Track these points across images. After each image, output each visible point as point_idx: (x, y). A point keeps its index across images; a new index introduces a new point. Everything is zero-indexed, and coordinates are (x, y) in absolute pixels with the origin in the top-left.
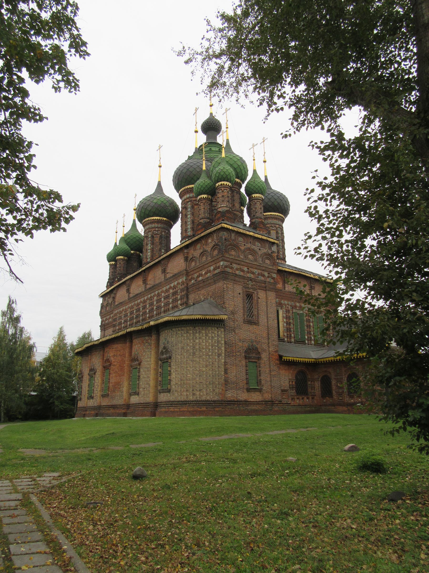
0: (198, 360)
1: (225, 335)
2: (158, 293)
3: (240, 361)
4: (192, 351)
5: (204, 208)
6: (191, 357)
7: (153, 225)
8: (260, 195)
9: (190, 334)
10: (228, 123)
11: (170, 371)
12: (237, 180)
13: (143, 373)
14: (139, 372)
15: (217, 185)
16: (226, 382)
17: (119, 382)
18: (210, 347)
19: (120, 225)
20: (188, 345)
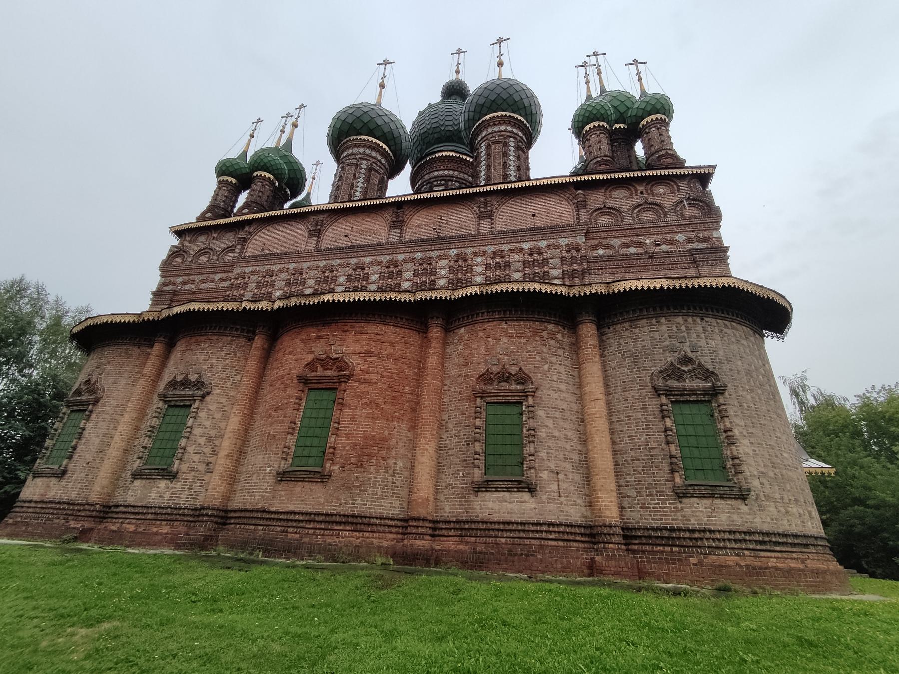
7: (373, 154)
17: (385, 440)
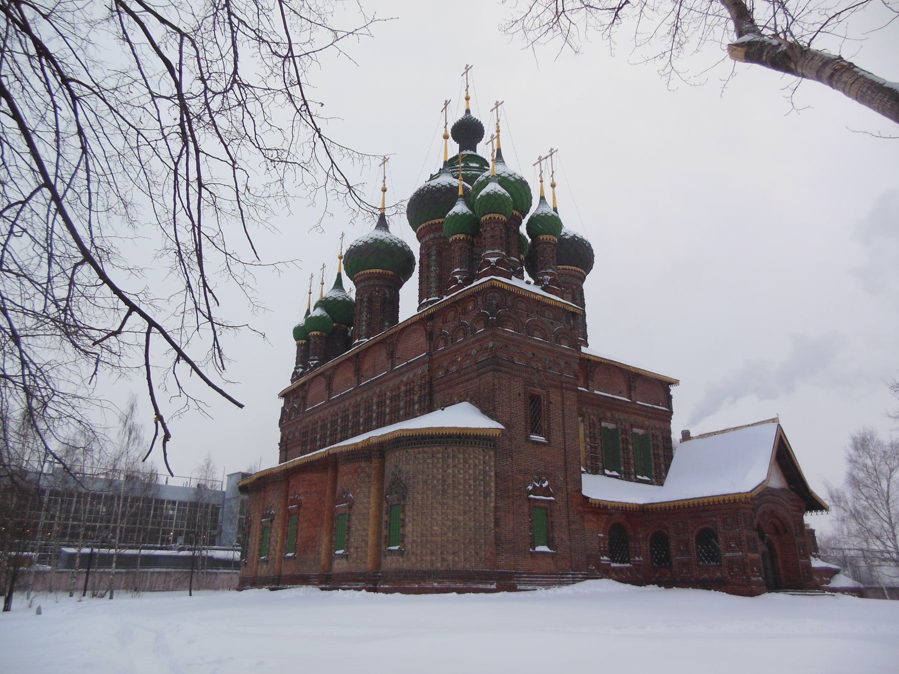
0: (451, 502)
1: (495, 463)
2: (381, 391)
4: (440, 487)
5: (461, 256)
6: (439, 497)
8: (552, 237)
9: (438, 459)
10: (500, 124)
11: (404, 520)
12: (515, 212)
13: (356, 522)
14: (349, 520)
15: (483, 218)
16: (498, 541)
18: (471, 482)
19: (317, 281)
20: (433, 477)
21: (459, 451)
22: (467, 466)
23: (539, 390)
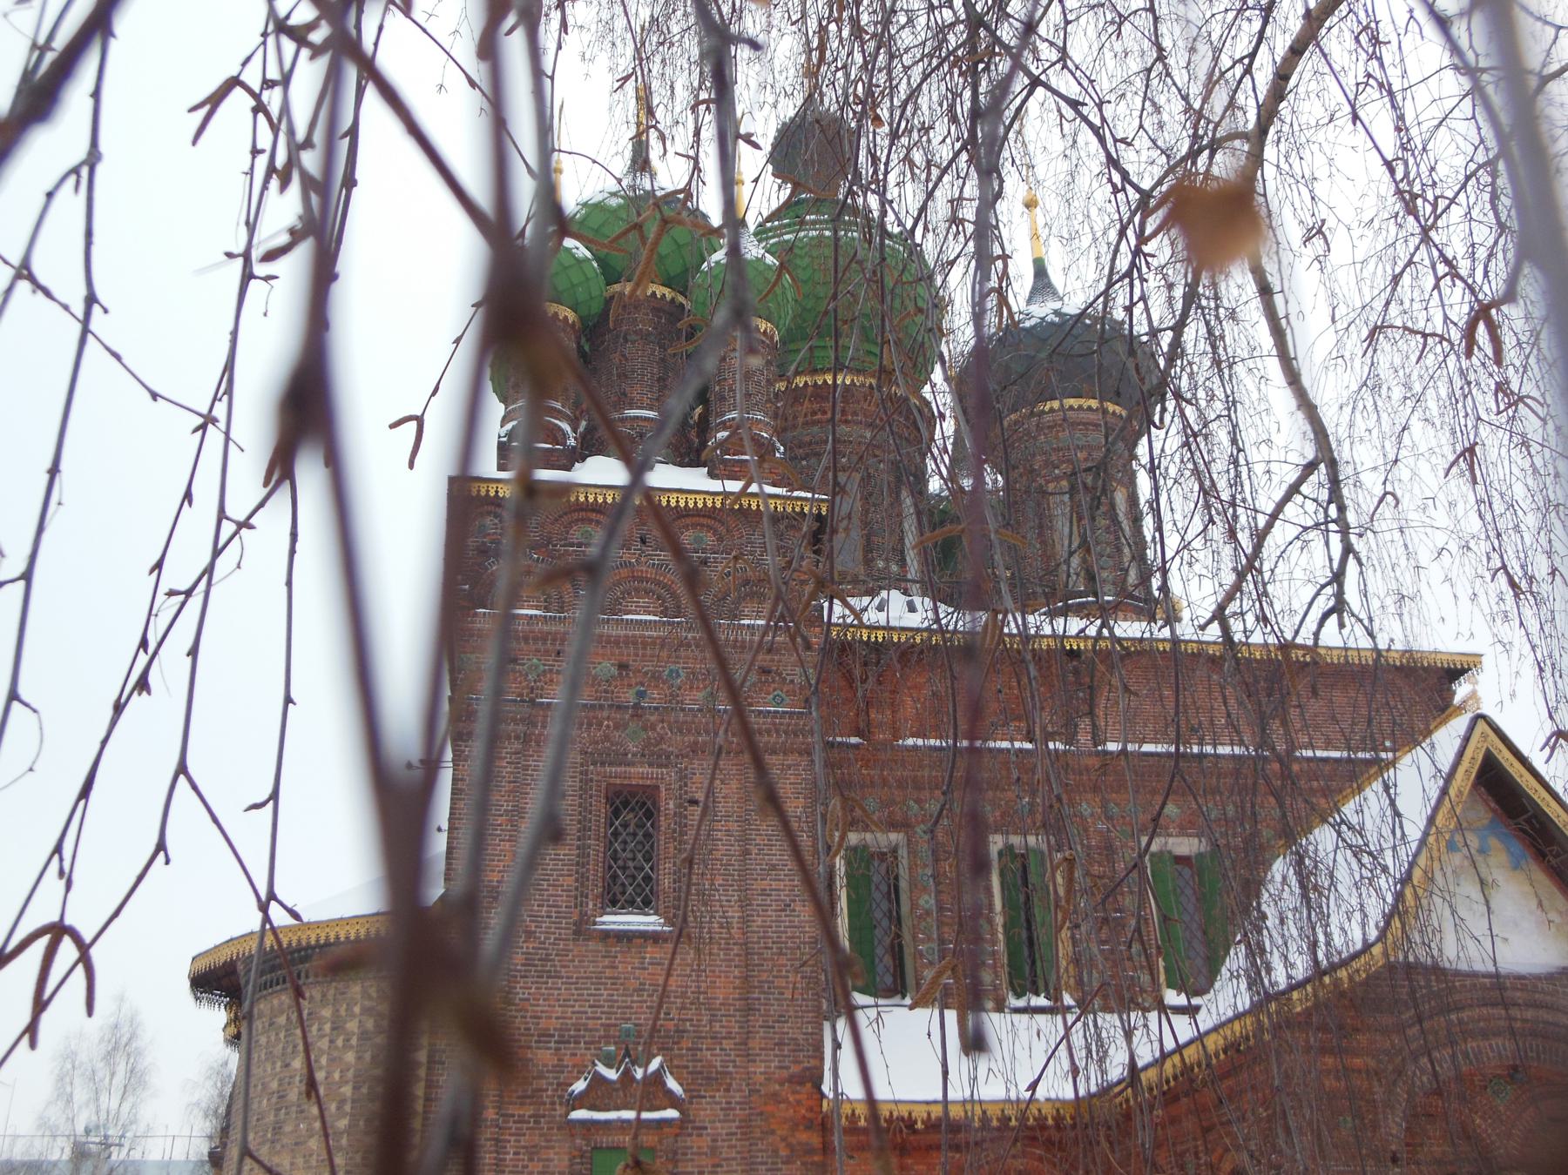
3: (532, 1151)
4: (272, 1118)
21: (324, 995)
22: (340, 1042)
23: (646, 770)
